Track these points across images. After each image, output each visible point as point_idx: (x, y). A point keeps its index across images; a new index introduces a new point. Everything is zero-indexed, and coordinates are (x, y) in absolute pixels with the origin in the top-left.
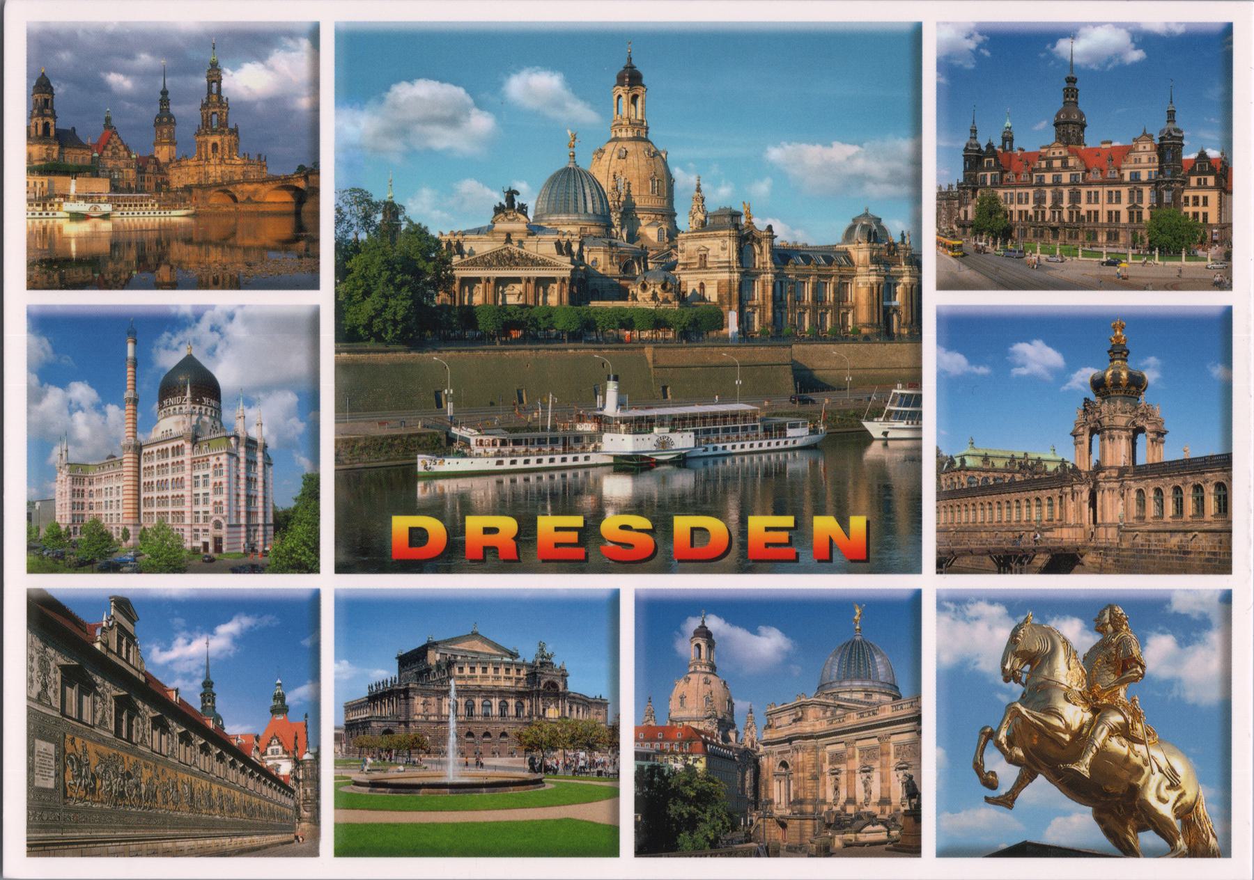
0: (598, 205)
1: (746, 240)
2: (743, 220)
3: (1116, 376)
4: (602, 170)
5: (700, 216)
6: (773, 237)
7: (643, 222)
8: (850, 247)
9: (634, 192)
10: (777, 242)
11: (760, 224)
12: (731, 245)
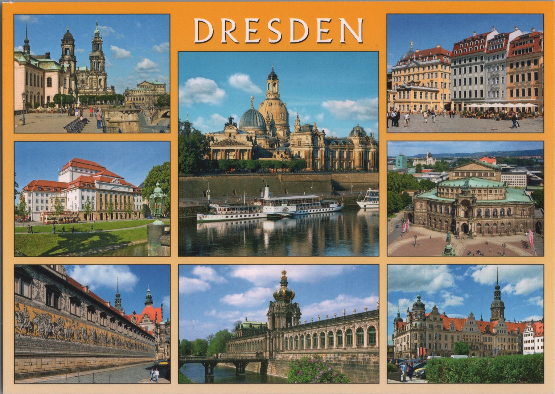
0: (262, 123)
1: (315, 136)
2: (314, 128)
3: (281, 292)
4: (263, 110)
5: (298, 127)
6: (324, 135)
7: (278, 129)
8: (352, 138)
9: (275, 118)
10: (326, 136)
11: (320, 130)
12: (310, 137)
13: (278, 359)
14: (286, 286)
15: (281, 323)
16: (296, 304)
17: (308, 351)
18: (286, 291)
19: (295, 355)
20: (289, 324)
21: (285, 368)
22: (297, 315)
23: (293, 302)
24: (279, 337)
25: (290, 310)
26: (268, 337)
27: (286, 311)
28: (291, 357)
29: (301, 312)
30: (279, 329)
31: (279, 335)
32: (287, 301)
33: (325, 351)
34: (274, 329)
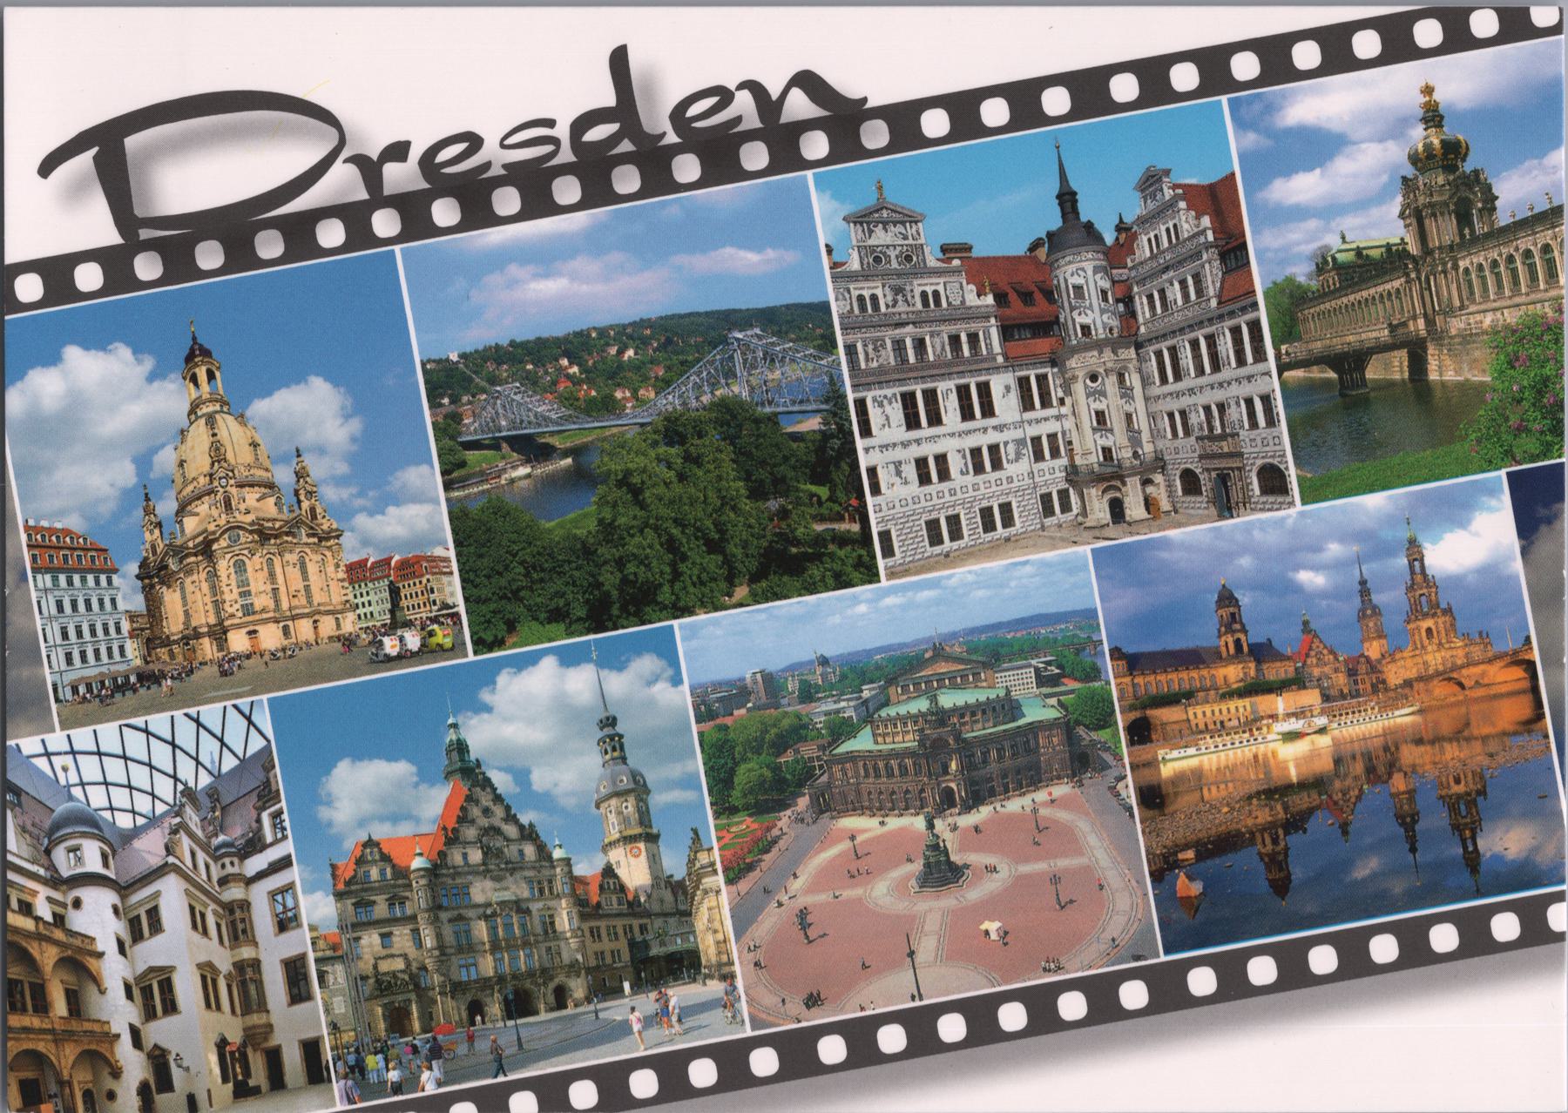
13: (1453, 332)
14: (1439, 126)
15: (1444, 231)
16: (1476, 172)
17: (1533, 297)
18: (1442, 142)
19: (1498, 314)
20: (1467, 231)
21: (1477, 354)
22: (1485, 202)
23: (1468, 167)
24: (1445, 272)
26: (1413, 275)
28: (1488, 320)
29: (1495, 191)
30: (1440, 248)
31: (1445, 264)
32: (1450, 168)
34: (1427, 251)
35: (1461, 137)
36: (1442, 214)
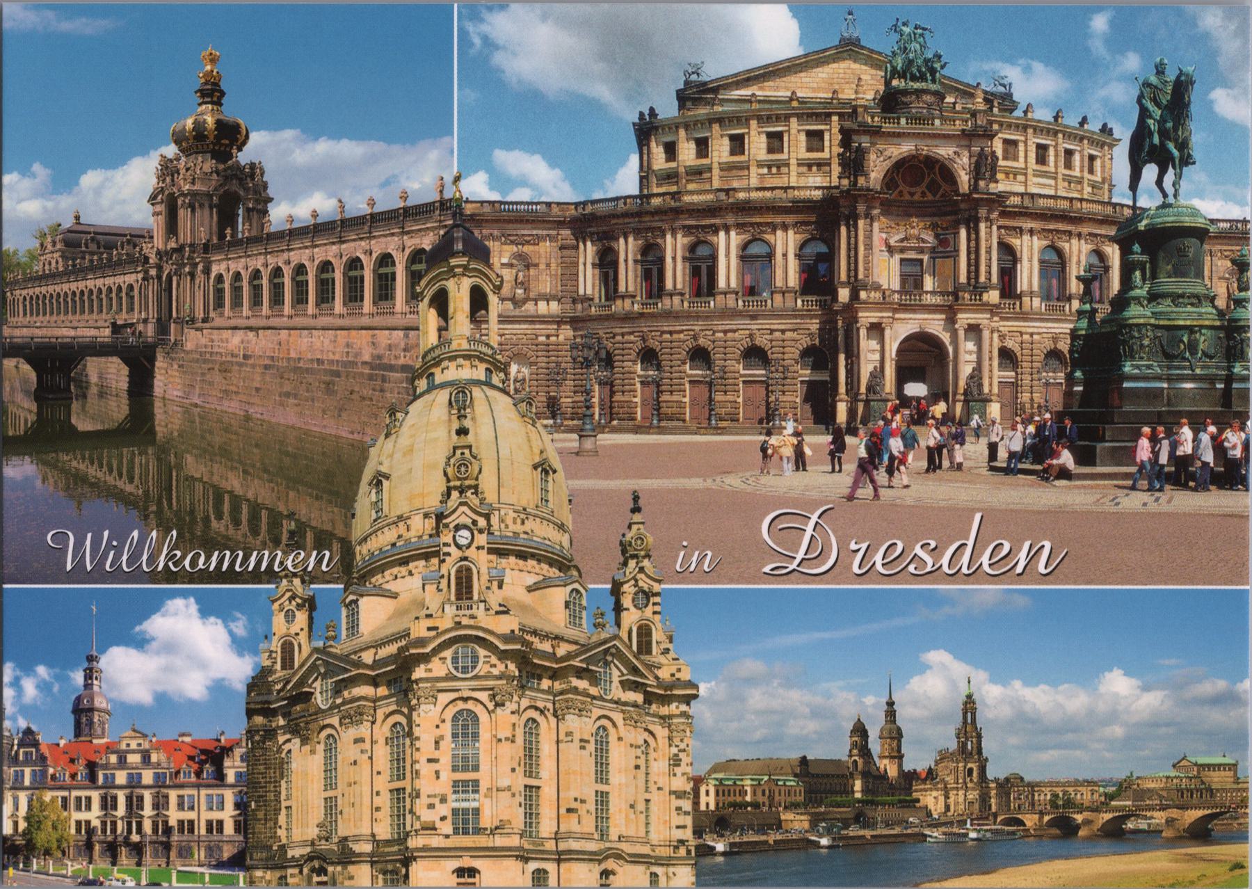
15: (197, 226)
16: (253, 166)
17: (298, 321)
18: (219, 123)
20: (228, 231)
23: (243, 157)
24: (192, 275)
25: (234, 186)
27: (216, 189)
29: (271, 192)
30: (191, 245)
32: (222, 155)
33: (365, 321)
35: (241, 122)
36: (201, 206)
